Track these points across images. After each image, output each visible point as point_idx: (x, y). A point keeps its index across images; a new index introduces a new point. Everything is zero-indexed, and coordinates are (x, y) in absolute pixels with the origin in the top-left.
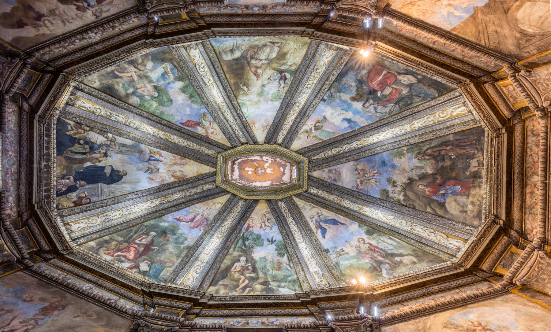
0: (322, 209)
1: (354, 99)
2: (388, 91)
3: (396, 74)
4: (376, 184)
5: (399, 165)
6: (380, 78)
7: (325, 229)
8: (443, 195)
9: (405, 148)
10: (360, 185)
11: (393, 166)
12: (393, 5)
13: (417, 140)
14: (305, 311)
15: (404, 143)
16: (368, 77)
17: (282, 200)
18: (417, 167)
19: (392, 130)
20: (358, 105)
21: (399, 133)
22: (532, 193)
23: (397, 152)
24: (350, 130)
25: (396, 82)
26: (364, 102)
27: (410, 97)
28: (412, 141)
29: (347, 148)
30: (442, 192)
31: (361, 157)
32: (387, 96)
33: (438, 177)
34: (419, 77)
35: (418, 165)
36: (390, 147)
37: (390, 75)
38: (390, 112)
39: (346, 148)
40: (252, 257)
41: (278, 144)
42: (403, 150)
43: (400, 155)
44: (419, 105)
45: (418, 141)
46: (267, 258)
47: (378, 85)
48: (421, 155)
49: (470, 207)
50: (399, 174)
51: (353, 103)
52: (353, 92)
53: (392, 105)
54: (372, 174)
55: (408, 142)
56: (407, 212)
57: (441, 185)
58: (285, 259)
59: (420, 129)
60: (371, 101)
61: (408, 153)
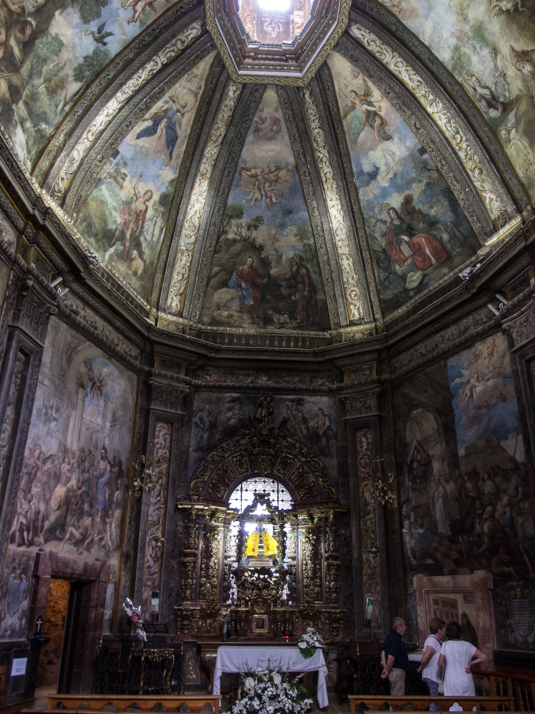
0: (194, 111)
1: (408, 200)
2: (406, 250)
3: (426, 272)
4: (251, 200)
5: (285, 233)
6: (428, 252)
7: (155, 131)
8: (240, 286)
9: (312, 242)
10: (249, 173)
11: (282, 226)
12: (502, 337)
13: (323, 259)
14: (21, 224)
15: (320, 242)
16: (435, 237)
17: (205, 31)
18: (281, 257)
19: (344, 230)
20: (396, 201)
21: (337, 238)
22: (249, 375)
23: (306, 231)
24: (355, 170)
25: (415, 267)
26: (399, 211)
27: (388, 269)
28: (322, 252)
29: (321, 155)
30: (243, 285)
31: (303, 178)
32: (399, 246)
33: (265, 281)
34: (412, 293)
35: (284, 258)
36: (317, 220)
37: (427, 265)
38: (374, 238)
39: (323, 154)
40: (54, 15)
41: (349, 26)
42: (308, 239)
43: (301, 235)
44: (374, 274)
45: (321, 260)
46: (63, 50)
47: (419, 245)
48: (299, 261)
49: (226, 313)
50: (270, 233)
51: (403, 196)
52: (421, 206)
53: (384, 244)
54: (269, 194)
55: (321, 247)
56: (208, 244)
57: (253, 284)
58: (74, 87)
59: (339, 266)
60: (397, 222)
61: (304, 246)
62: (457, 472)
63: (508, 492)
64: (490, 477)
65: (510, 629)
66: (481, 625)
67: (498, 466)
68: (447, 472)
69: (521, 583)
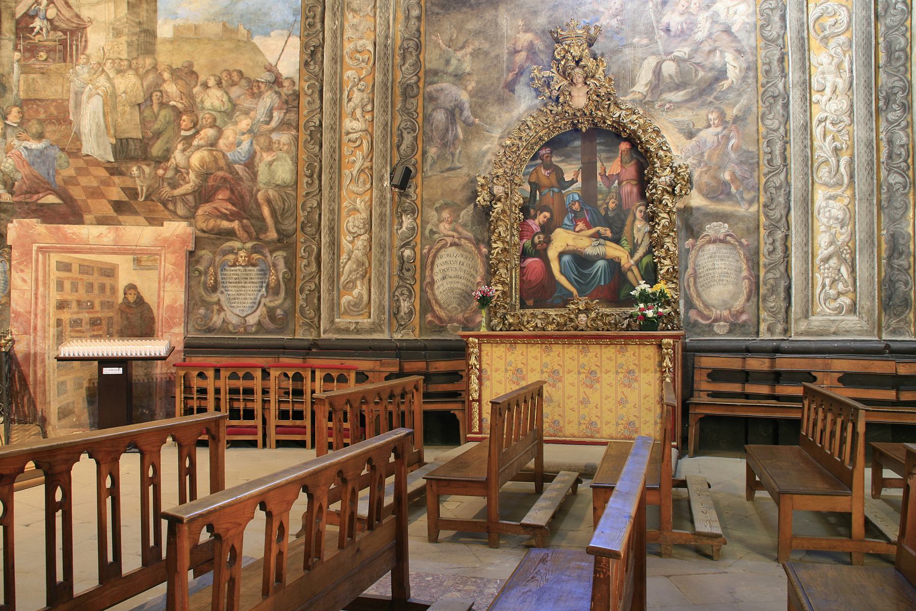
62: (149, 61)
63: (252, 114)
64: (219, 84)
65: (216, 307)
66: (167, 301)
67: (240, 72)
68: (124, 56)
69: (249, 245)
